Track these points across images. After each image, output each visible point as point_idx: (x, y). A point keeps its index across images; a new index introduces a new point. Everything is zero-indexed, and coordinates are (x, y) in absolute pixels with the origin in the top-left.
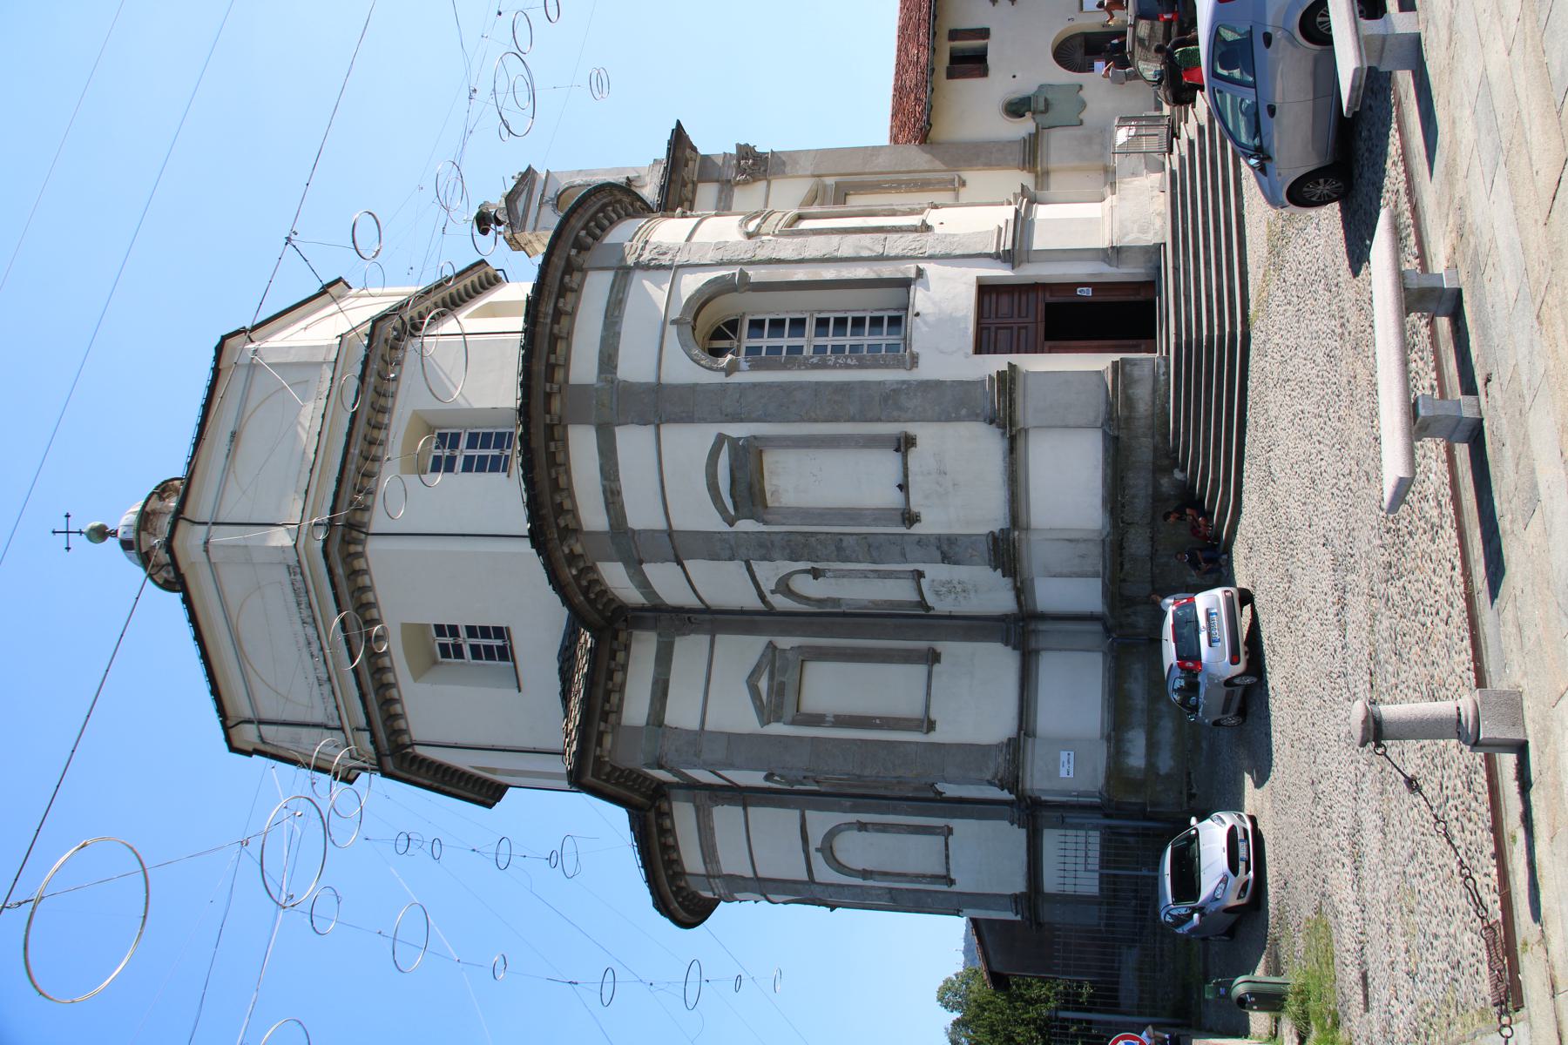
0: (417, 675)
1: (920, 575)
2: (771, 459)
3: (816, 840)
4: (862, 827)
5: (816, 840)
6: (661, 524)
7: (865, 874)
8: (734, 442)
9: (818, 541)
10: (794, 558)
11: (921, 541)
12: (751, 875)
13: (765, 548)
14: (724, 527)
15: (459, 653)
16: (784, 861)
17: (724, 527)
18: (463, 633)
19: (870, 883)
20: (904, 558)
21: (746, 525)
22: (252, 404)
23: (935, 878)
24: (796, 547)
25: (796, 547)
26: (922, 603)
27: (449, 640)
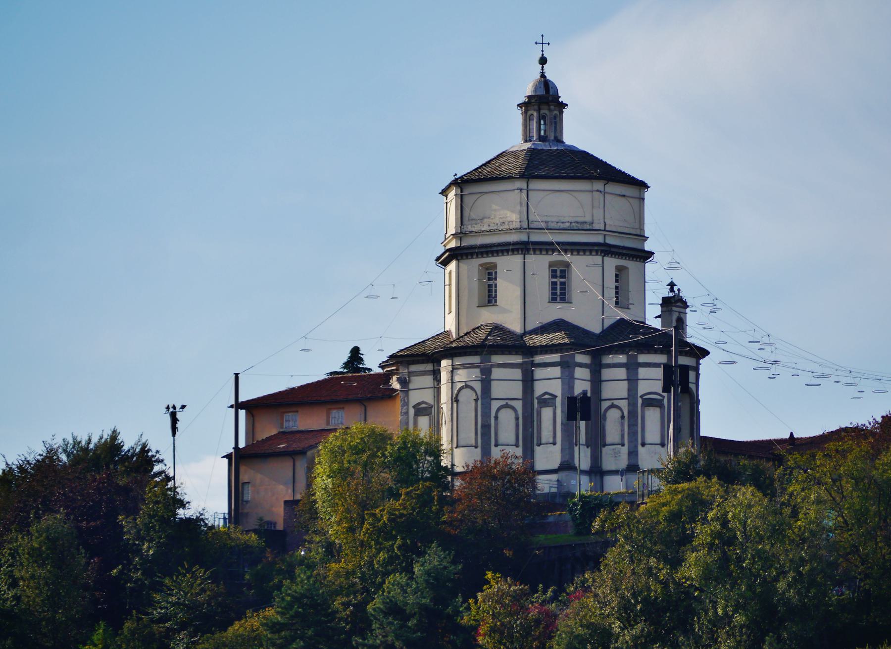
0: (551, 265)
1: (623, 445)
2: (658, 410)
3: (510, 403)
4: (517, 419)
5: (510, 403)
6: (640, 377)
7: (496, 418)
8: (663, 400)
9: (633, 420)
10: (629, 412)
11: (636, 447)
12: (492, 377)
13: (632, 405)
14: (639, 395)
15: (554, 277)
16: (498, 390)
17: (639, 395)
18: (562, 280)
19: (493, 420)
20: (629, 442)
21: (640, 401)
22: (630, 200)
23: (496, 440)
24: (633, 414)
25: (633, 414)
26: (605, 445)
27: (558, 274)
